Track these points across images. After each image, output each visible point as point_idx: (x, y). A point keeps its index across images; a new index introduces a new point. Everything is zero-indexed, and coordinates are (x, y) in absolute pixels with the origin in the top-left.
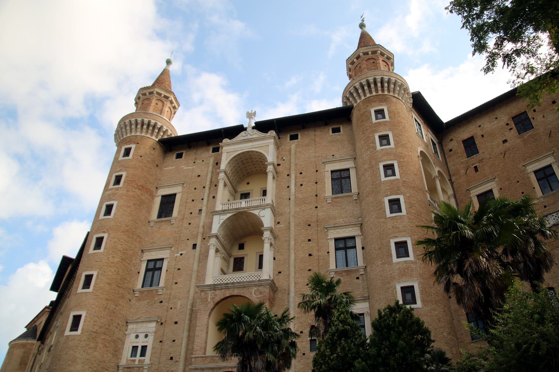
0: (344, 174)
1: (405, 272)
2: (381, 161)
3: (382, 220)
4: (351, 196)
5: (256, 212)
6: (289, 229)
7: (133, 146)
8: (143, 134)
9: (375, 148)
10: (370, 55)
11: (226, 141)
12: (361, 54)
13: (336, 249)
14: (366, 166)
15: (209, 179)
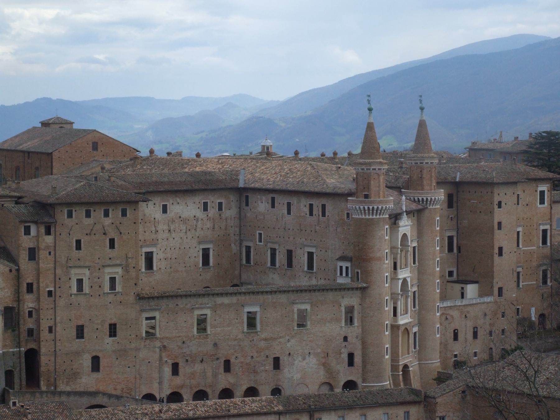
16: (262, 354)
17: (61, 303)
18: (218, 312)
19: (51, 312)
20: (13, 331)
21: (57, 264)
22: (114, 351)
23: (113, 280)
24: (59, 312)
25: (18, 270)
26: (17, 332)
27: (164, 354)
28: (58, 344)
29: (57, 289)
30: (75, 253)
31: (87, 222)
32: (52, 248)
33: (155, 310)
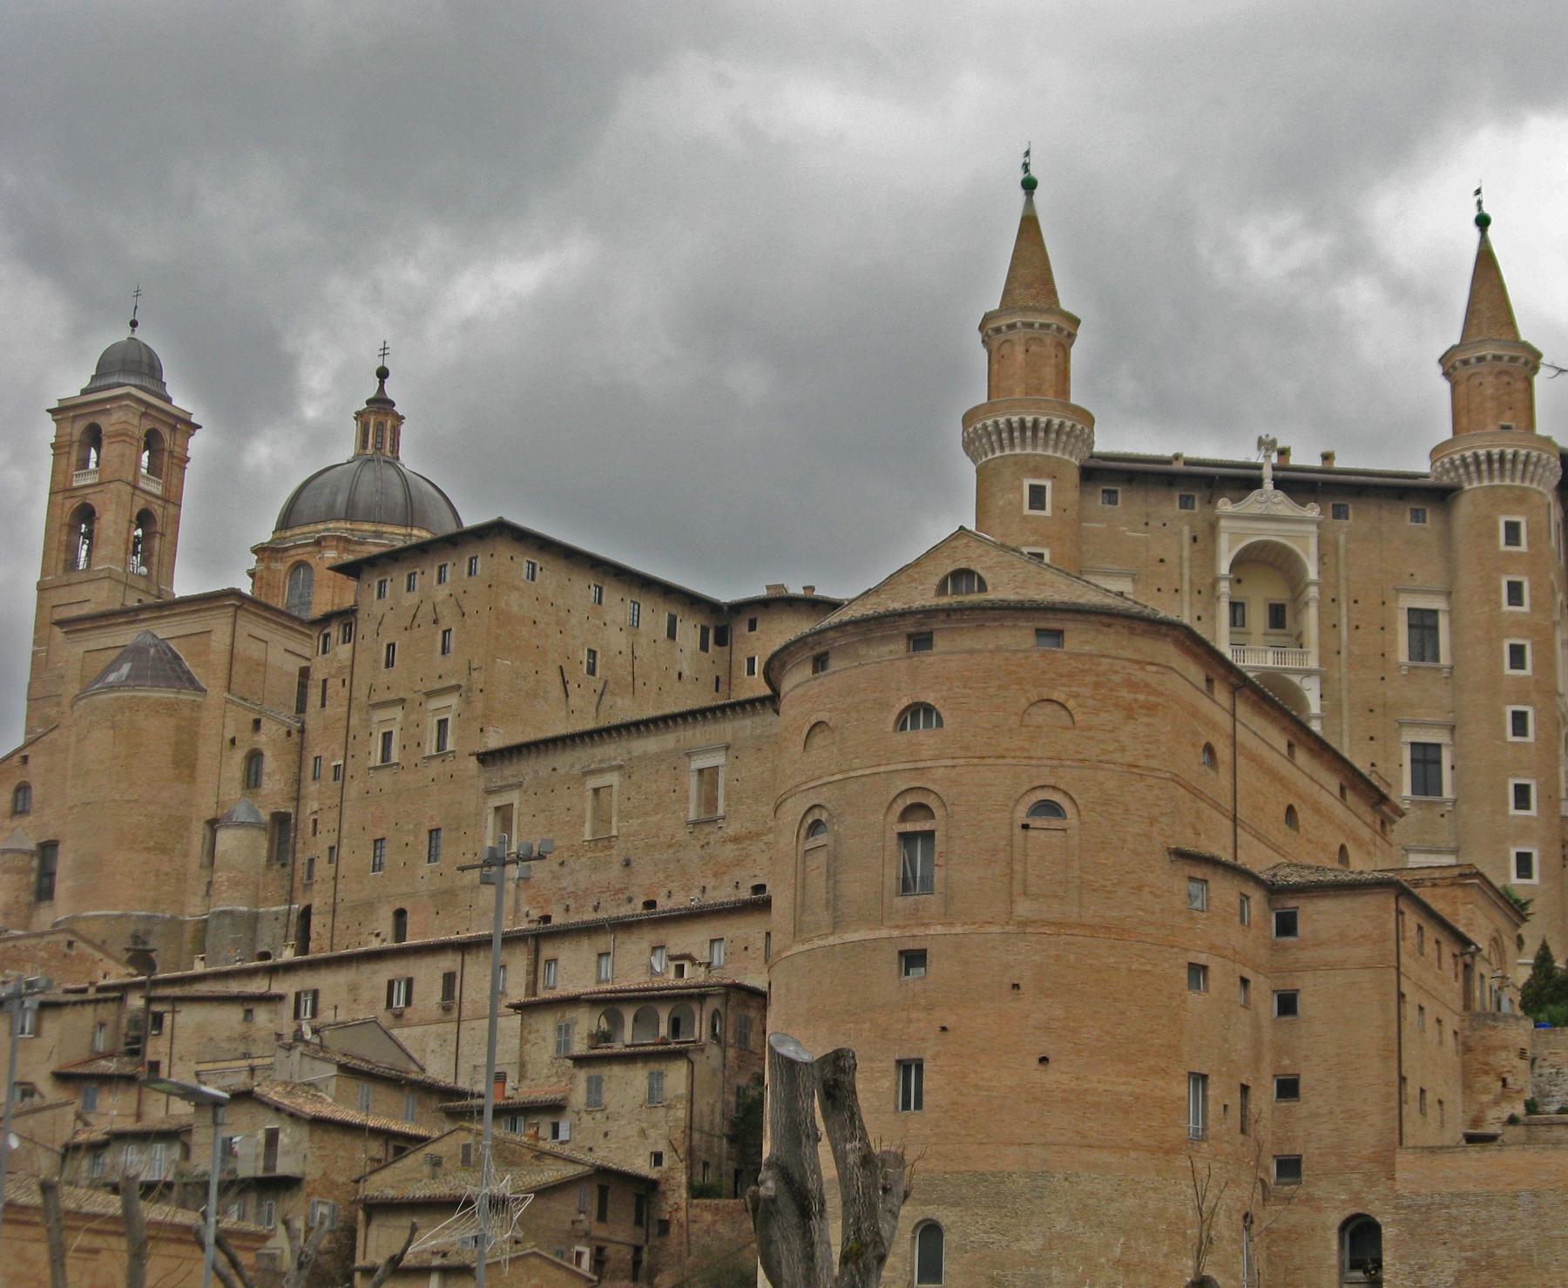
0: (1428, 622)
1: (1524, 830)
2: (1508, 636)
3: (1499, 743)
4: (1439, 670)
5: (1296, 679)
6: (1340, 712)
7: (1048, 484)
8: (1059, 455)
9: (1498, 604)
10: (1504, 365)
11: (1224, 505)
12: (1489, 357)
13: (1413, 761)
14: (1480, 633)
15: (1186, 578)
16: (726, 878)
17: (353, 790)
18: (634, 777)
19: (335, 814)
20: (283, 865)
21: (354, 703)
22: (433, 895)
23: (442, 724)
24: (347, 812)
25: (302, 731)
26: (289, 869)
27: (523, 896)
28: (340, 886)
29: (349, 761)
30: (385, 676)
31: (410, 599)
32: (348, 670)
33: (511, 787)
